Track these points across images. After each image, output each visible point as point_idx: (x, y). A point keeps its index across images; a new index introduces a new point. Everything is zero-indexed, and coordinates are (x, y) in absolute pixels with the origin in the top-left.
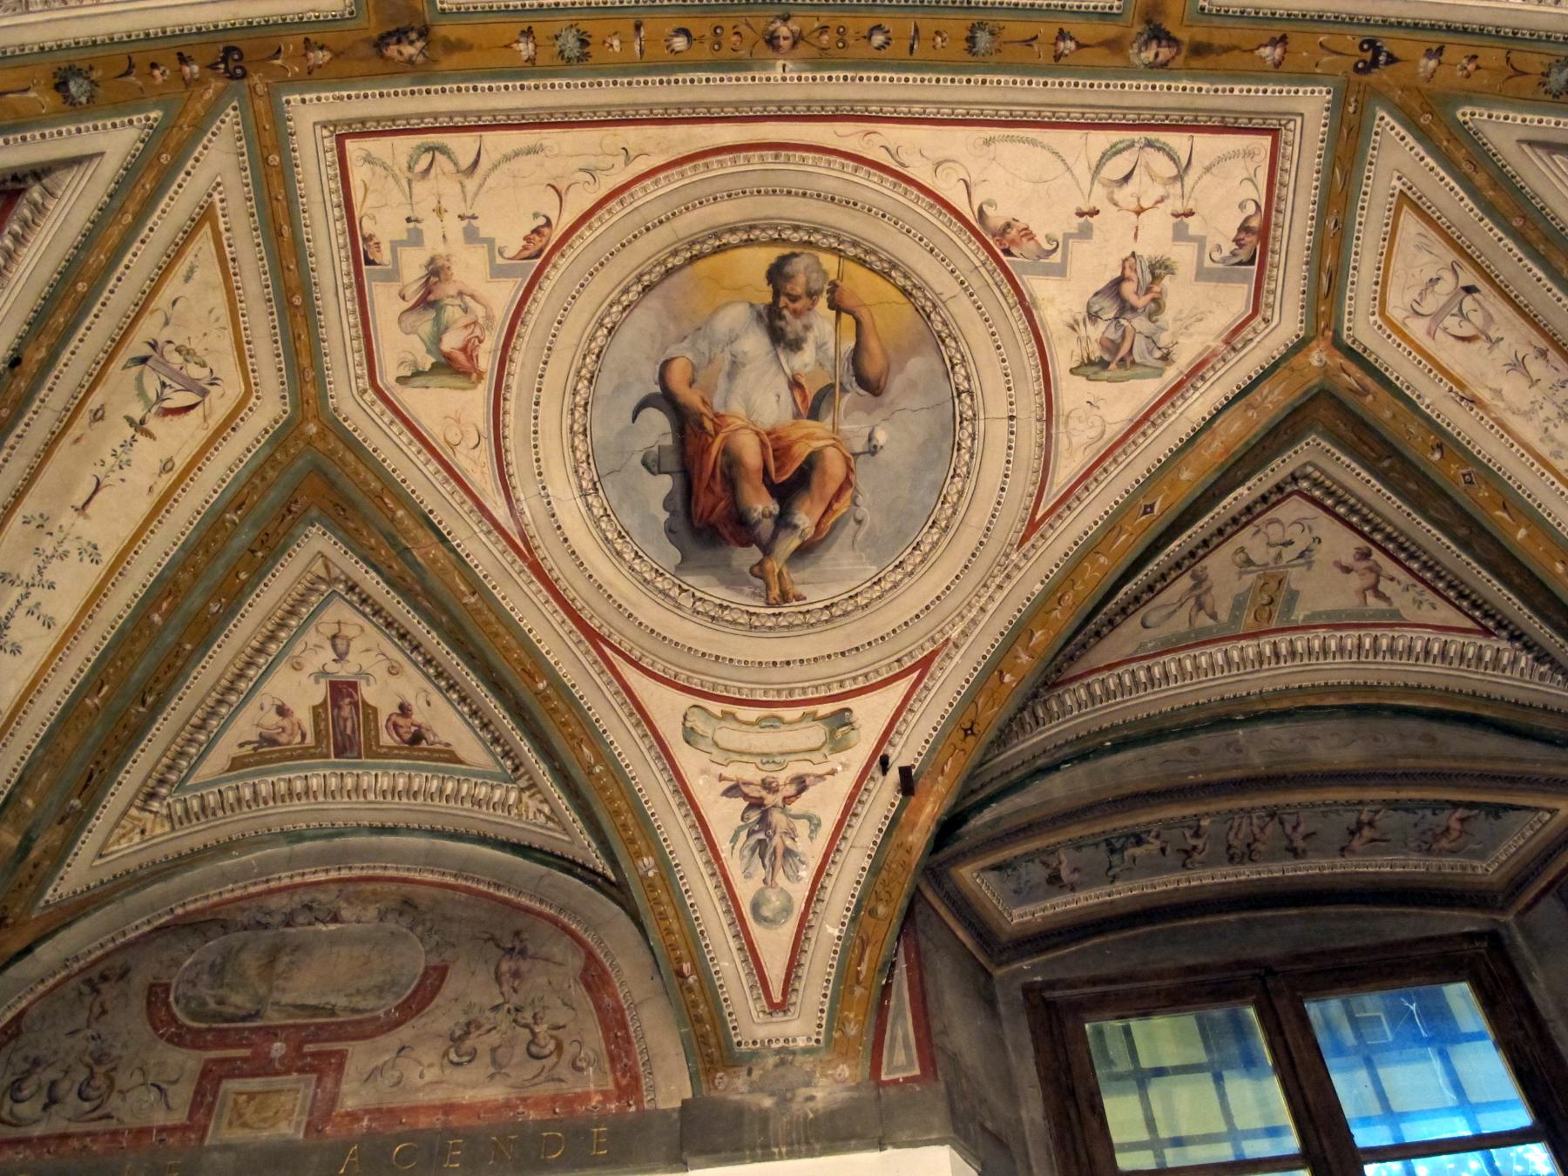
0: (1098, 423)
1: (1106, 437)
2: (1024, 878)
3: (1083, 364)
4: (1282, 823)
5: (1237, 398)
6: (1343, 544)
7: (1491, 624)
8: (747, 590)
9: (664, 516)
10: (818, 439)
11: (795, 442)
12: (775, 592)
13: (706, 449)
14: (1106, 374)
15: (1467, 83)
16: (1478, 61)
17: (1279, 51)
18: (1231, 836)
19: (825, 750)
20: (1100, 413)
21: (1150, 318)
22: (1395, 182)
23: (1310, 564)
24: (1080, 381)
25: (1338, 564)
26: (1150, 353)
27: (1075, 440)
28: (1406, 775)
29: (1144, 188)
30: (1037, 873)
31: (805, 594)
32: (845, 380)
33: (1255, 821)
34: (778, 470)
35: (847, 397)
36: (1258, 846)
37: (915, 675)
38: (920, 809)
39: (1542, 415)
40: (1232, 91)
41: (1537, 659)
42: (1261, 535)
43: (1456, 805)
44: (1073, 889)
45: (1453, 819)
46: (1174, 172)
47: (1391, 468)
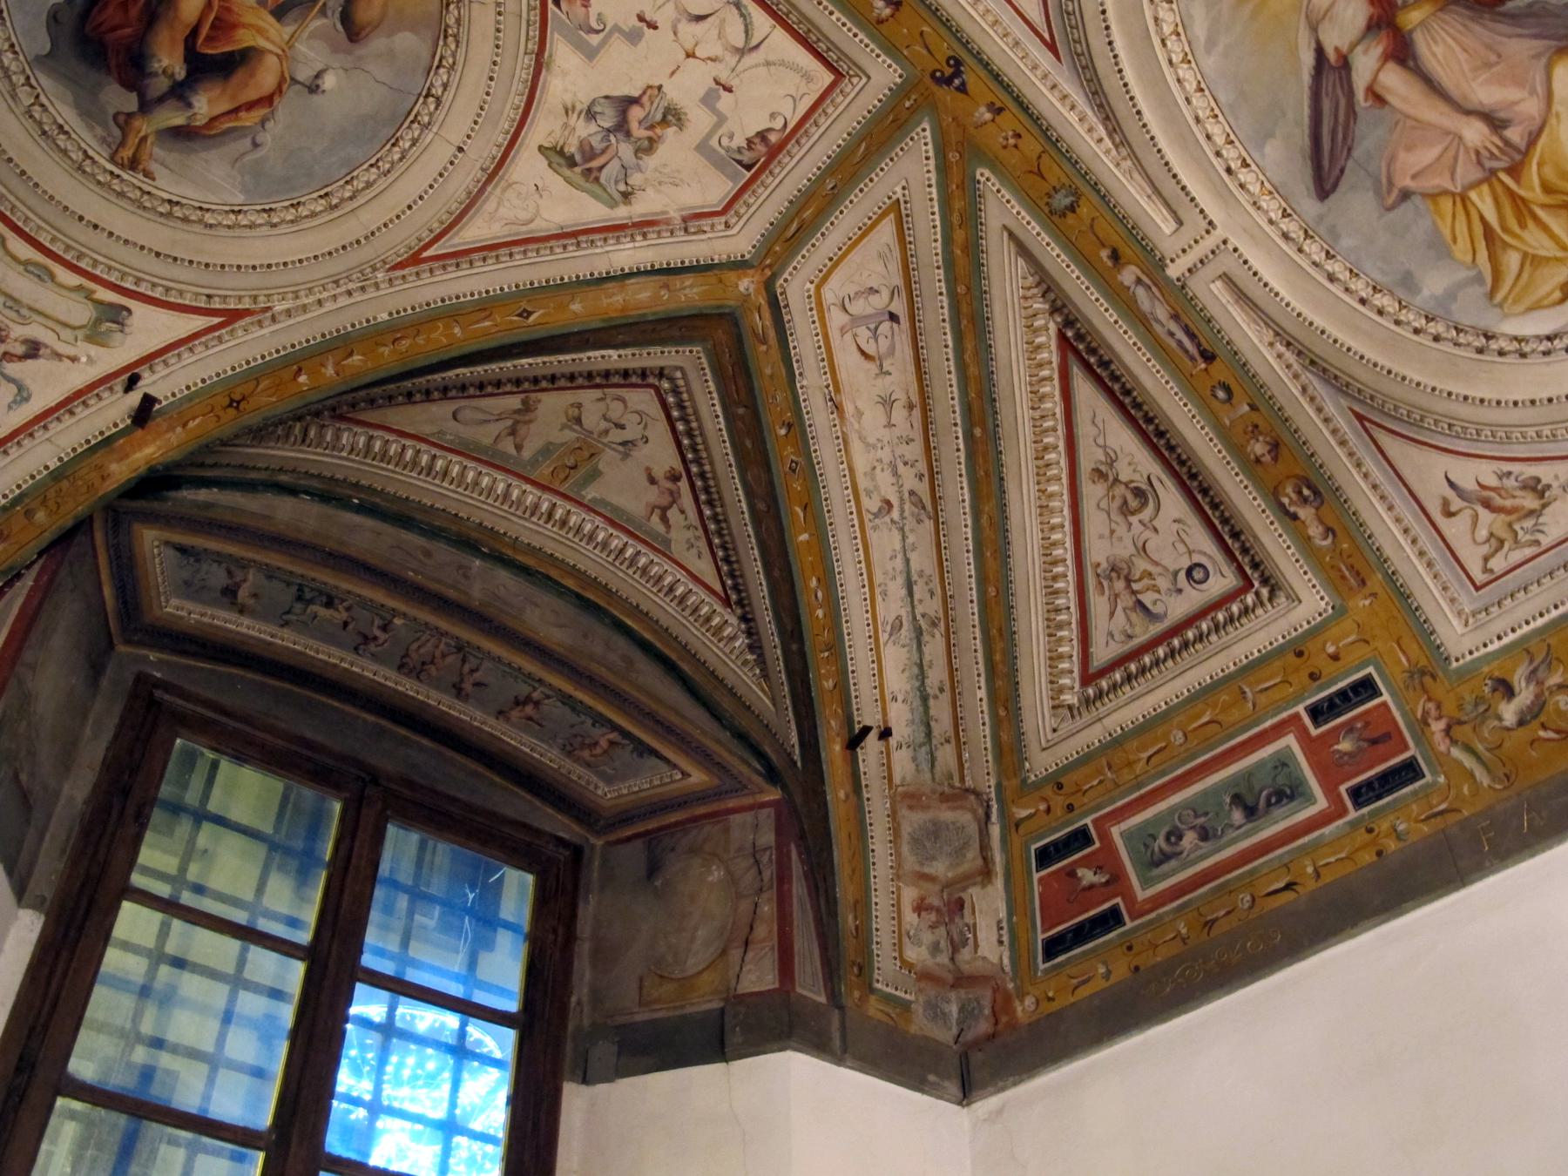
1: (532, 226)
3: (553, 149)
4: (464, 661)
5: (661, 272)
6: (661, 454)
7: (734, 597)
8: (99, 131)
10: (268, 39)
11: (244, 26)
12: (127, 153)
14: (567, 172)
15: (1003, 154)
16: (1020, 142)
17: (888, 11)
18: (415, 646)
19: (80, 334)
20: (540, 202)
21: (637, 151)
22: (898, 189)
23: (626, 456)
24: (542, 163)
25: (648, 471)
26: (616, 182)
27: (503, 211)
28: (591, 678)
29: (706, 38)
30: (217, 577)
32: (330, 4)
33: (442, 646)
34: (209, 39)
35: (317, 23)
36: (433, 669)
37: (216, 320)
38: (145, 444)
39: (880, 454)
40: (831, 13)
42: (601, 405)
43: (615, 728)
44: (241, 612)
45: (604, 738)
46: (740, 44)
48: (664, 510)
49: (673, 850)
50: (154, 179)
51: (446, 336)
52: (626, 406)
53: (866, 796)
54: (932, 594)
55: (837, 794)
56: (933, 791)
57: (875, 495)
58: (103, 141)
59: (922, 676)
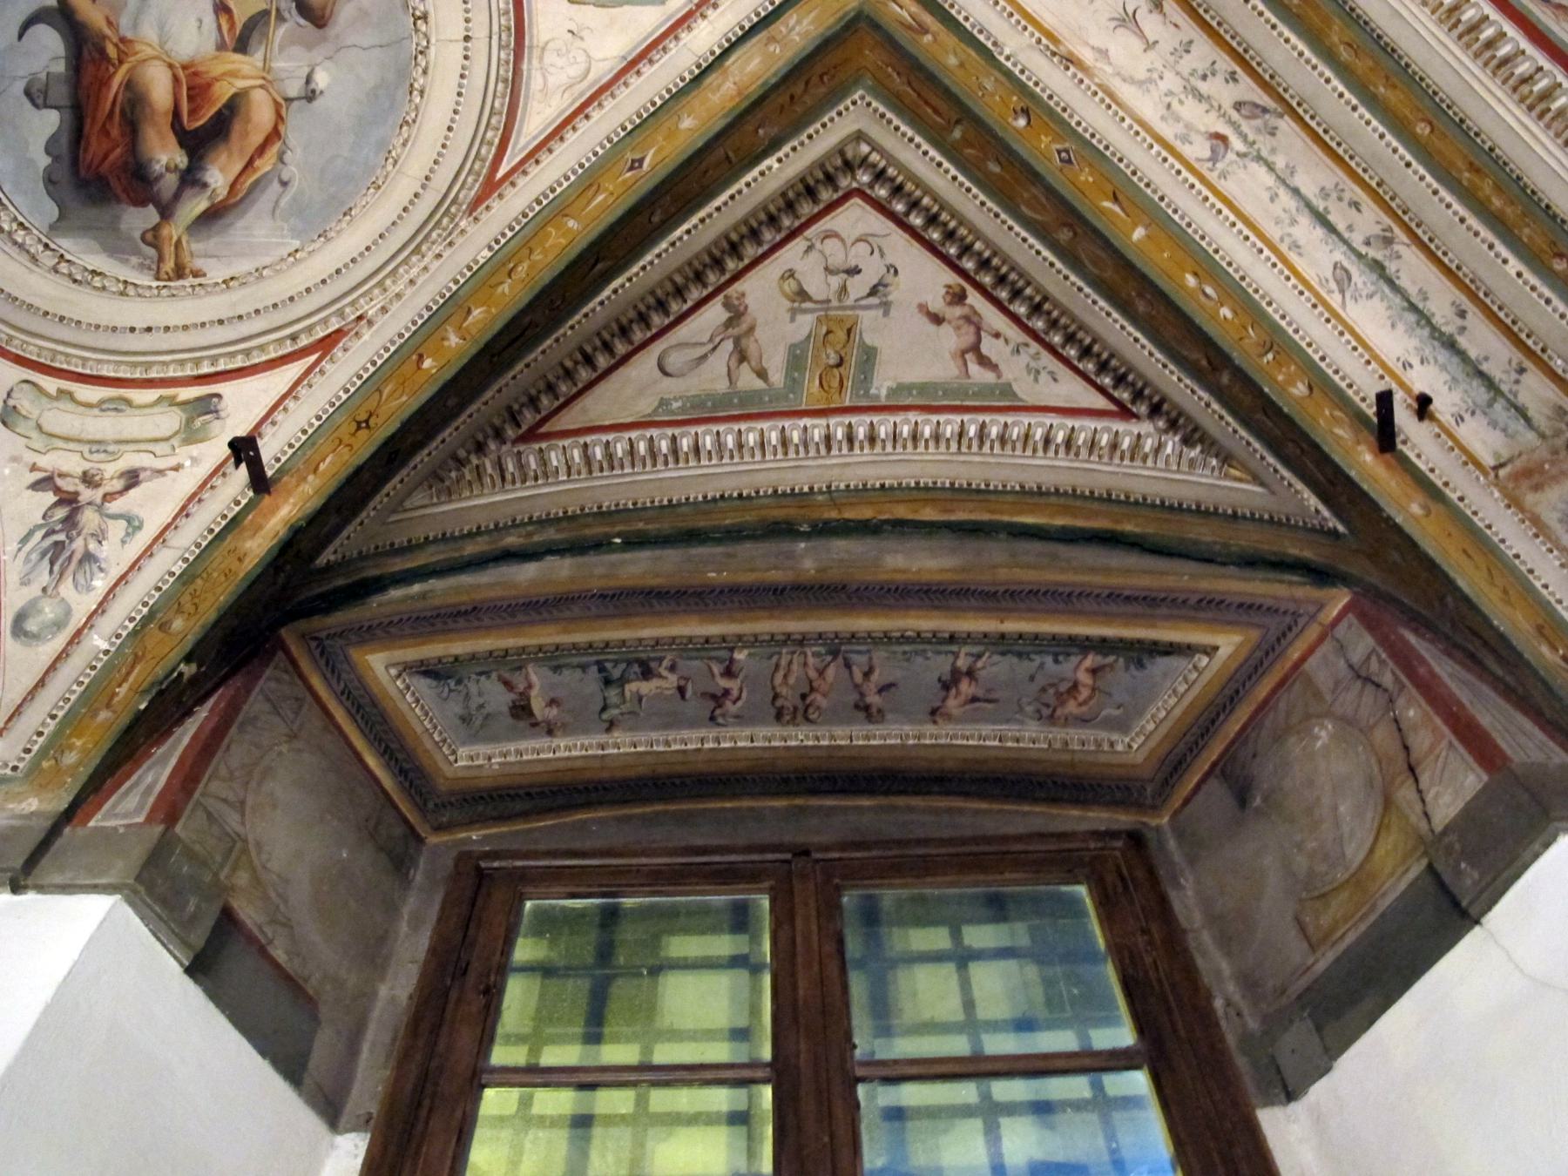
0: (581, 58)
1: (591, 77)
4: (848, 666)
6: (924, 278)
7: (1125, 396)
8: (134, 260)
9: (44, 161)
12: (169, 265)
13: (105, 82)
19: (175, 442)
20: (583, 45)
23: (886, 306)
25: (923, 309)
27: (551, 80)
28: (1013, 595)
30: (496, 697)
31: (205, 270)
32: (283, 5)
33: (811, 660)
35: (282, 30)
36: (817, 698)
38: (274, 510)
39: (1163, 86)
42: (814, 255)
43: (1085, 645)
44: (550, 733)
45: (1080, 668)
47: (965, 141)
48: (975, 348)
49: (1254, 756)
50: (204, 275)
51: (563, 235)
53: (1454, 496)
54: (1356, 205)
55: (1409, 511)
56: (1555, 452)
57: (1193, 137)
58: (142, 267)
59: (1424, 319)
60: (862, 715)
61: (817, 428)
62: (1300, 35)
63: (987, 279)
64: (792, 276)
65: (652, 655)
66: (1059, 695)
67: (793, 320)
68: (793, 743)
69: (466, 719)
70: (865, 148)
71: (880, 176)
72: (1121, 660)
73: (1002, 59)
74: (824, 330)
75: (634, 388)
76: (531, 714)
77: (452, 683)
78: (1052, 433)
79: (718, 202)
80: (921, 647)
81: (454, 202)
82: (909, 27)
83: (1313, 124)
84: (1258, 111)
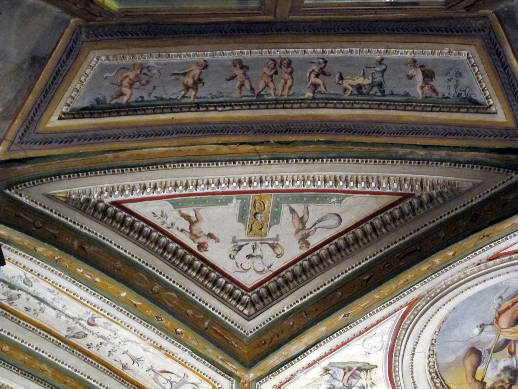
1: (362, 339)
2: (453, 83)
3: (370, 370)
4: (252, 89)
5: (293, 358)
6: (217, 254)
7: (121, 214)
10: (508, 332)
14: (359, 365)
23: (234, 241)
24: (372, 363)
25: (217, 240)
26: (335, 372)
27: (379, 338)
28: (169, 133)
30: (440, 84)
32: (487, 354)
35: (489, 347)
39: (118, 340)
41: (88, 201)
42: (268, 264)
44: (414, 61)
45: (130, 95)
47: (203, 321)
48: (192, 224)
52: (255, 270)
54: (27, 309)
60: (244, 64)
61: (266, 186)
62: (64, 369)
63: (189, 257)
64: (278, 255)
65: (355, 97)
66: (139, 80)
67: (278, 235)
68: (282, 50)
69: (459, 74)
70: (246, 312)
71: (239, 300)
72: (108, 102)
73: (189, 350)
74: (263, 230)
75: (354, 210)
76: (423, 72)
77: (463, 95)
78: (154, 194)
79: (311, 296)
80: (215, 100)
81: (428, 302)
82: (228, 362)
83: (52, 338)
84: (77, 336)
